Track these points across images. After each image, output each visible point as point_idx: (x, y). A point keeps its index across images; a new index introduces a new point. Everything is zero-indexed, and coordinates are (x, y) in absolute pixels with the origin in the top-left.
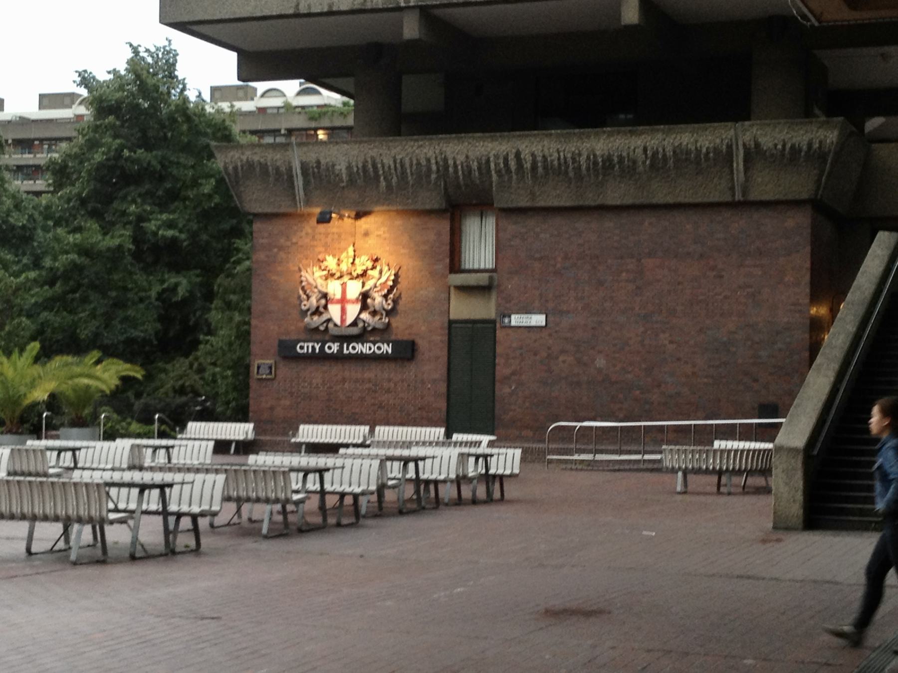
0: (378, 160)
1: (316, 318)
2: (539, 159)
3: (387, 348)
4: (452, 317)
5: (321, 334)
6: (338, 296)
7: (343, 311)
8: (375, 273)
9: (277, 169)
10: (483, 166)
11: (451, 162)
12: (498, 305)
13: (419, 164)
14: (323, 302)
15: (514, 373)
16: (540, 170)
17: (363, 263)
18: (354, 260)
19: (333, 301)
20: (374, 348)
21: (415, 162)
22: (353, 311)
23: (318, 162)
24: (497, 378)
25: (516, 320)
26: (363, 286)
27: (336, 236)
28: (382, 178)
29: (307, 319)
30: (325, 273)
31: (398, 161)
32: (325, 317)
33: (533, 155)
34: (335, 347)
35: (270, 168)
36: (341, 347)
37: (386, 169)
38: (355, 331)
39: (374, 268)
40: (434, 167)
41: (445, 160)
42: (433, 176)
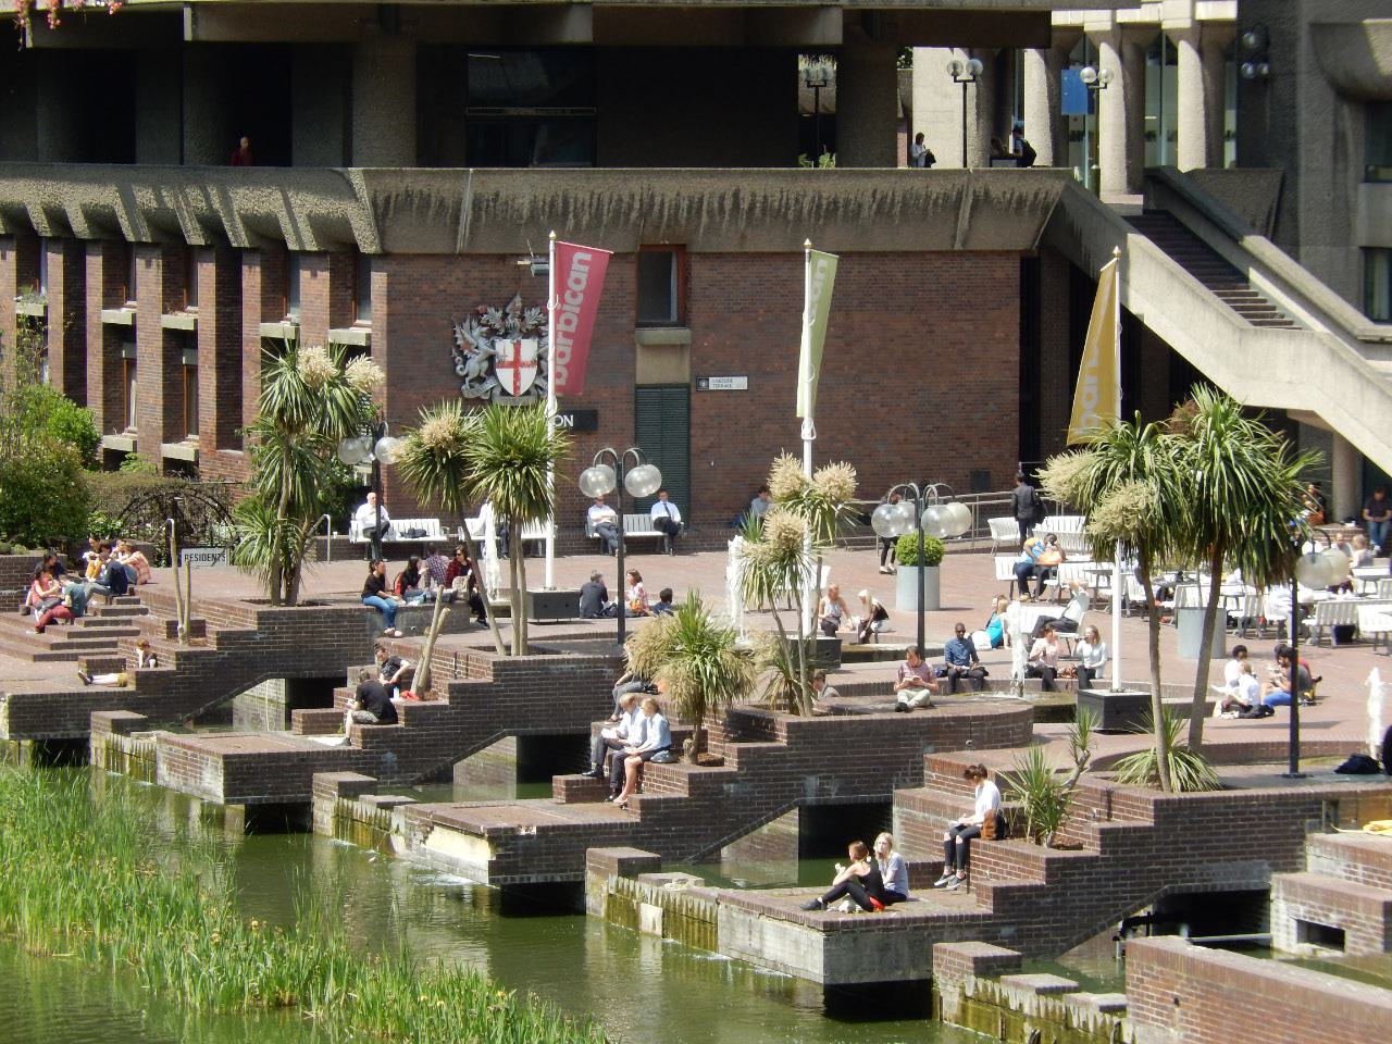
0: (572, 194)
1: (477, 385)
2: (759, 199)
4: (640, 380)
6: (510, 358)
7: (517, 376)
9: (442, 202)
10: (695, 206)
11: (658, 200)
12: (692, 366)
13: (621, 200)
14: (485, 365)
16: (758, 211)
18: (523, 312)
19: (503, 365)
21: (615, 197)
23: (497, 195)
24: (693, 451)
25: (715, 383)
26: (539, 347)
27: (495, 283)
28: (571, 216)
30: (485, 329)
31: (596, 196)
33: (754, 195)
35: (433, 199)
37: (579, 205)
40: (637, 205)
41: (652, 197)
42: (634, 215)
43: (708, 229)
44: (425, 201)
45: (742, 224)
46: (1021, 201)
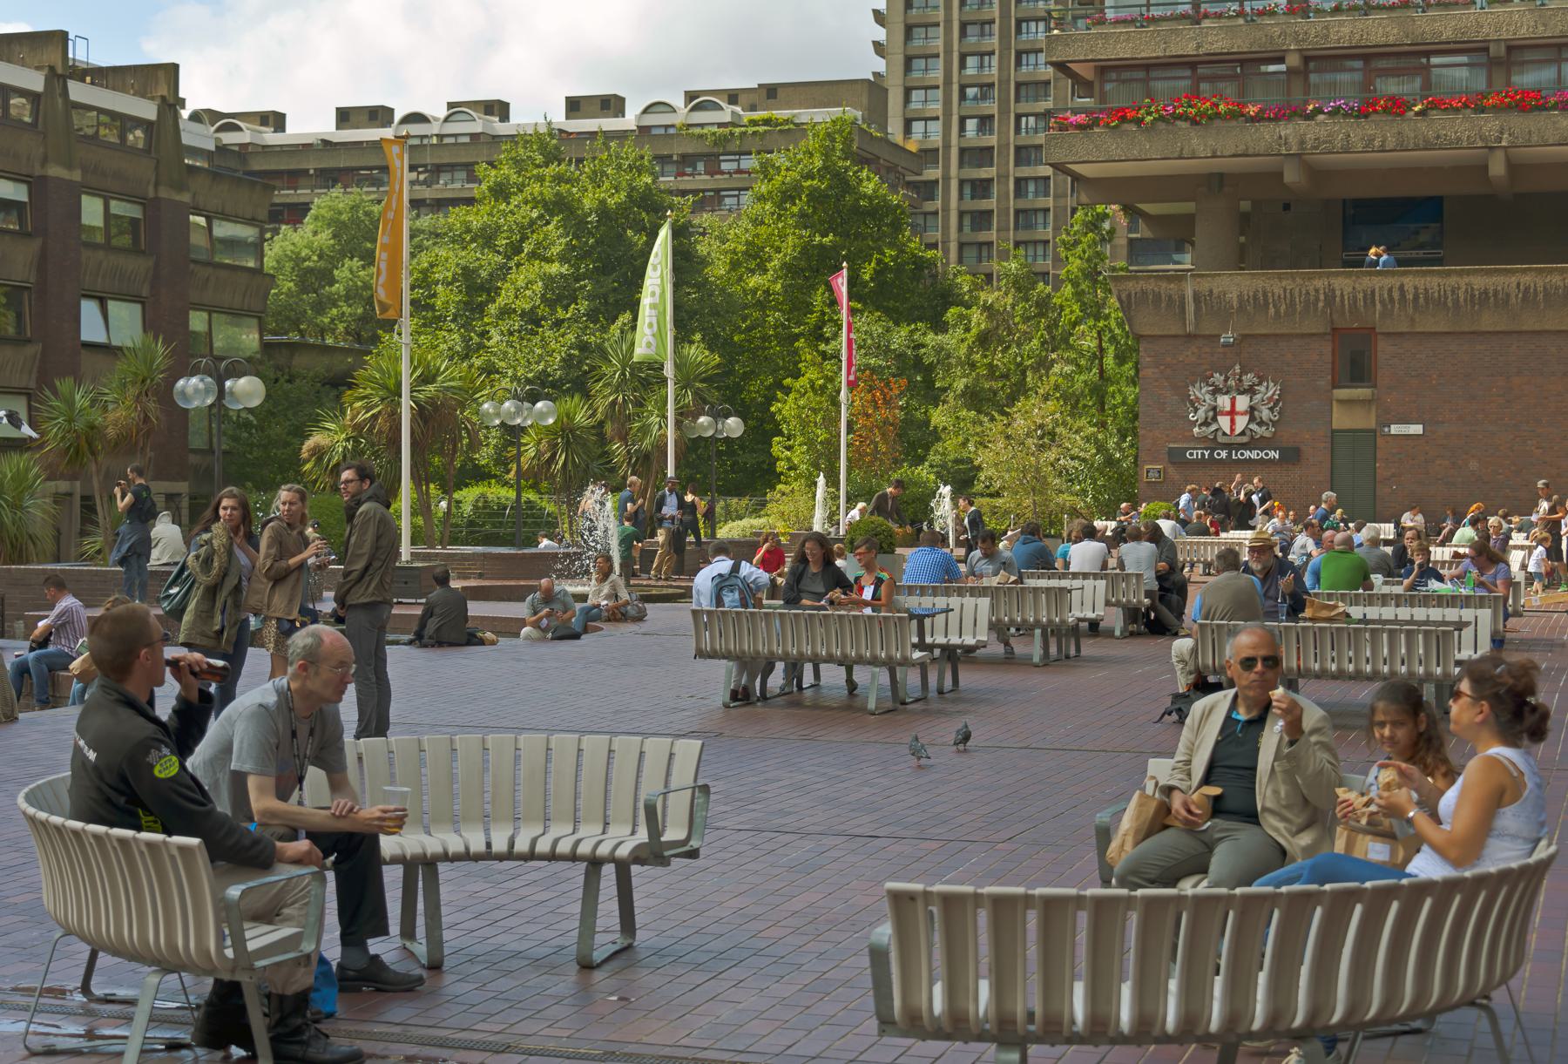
4: (1335, 426)
5: (1213, 443)
6: (1228, 408)
7: (1233, 422)
8: (1263, 389)
11: (1338, 293)
12: (1378, 417)
15: (1393, 475)
17: (1249, 379)
20: (1262, 455)
22: (1242, 422)
25: (1395, 429)
29: (1196, 430)
32: (1213, 427)
33: (1416, 288)
34: (1224, 454)
36: (1230, 454)
38: (1245, 439)
39: (1260, 384)
40: (1322, 297)
41: (1333, 290)
42: (1321, 304)
43: (1383, 315)
44: (1157, 297)
45: (1411, 311)
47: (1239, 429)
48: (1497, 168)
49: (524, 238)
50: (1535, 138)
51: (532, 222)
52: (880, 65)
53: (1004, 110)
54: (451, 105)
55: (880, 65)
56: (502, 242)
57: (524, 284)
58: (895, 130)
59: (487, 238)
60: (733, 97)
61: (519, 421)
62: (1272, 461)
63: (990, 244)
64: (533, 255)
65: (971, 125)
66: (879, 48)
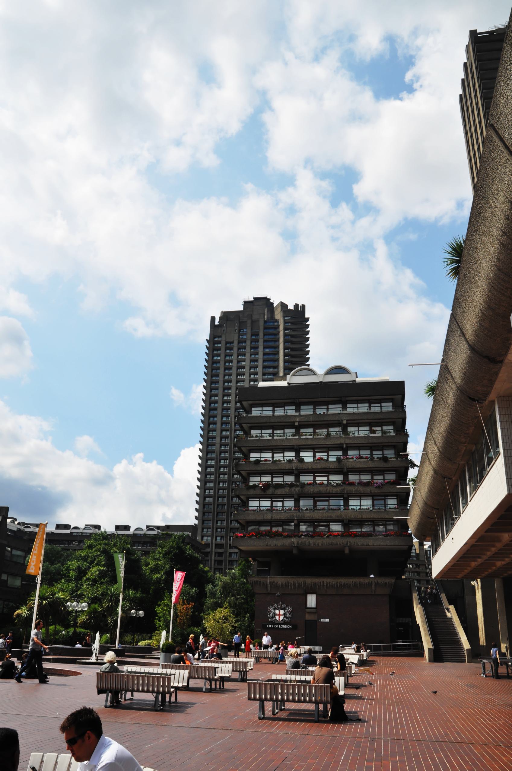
3: (290, 627)
7: (279, 617)
19: (277, 615)
25: (322, 620)
38: (282, 622)
46: (386, 583)
47: (281, 619)
48: (347, 551)
49: (95, 559)
50: (356, 544)
51: (97, 555)
52: (196, 522)
53: (227, 534)
54: (86, 525)
55: (196, 522)
56: (89, 560)
57: (94, 572)
58: (199, 538)
59: (85, 559)
60: (158, 527)
61: (77, 608)
62: (290, 628)
63: (222, 569)
64: (97, 564)
65: (219, 538)
66: (196, 518)
